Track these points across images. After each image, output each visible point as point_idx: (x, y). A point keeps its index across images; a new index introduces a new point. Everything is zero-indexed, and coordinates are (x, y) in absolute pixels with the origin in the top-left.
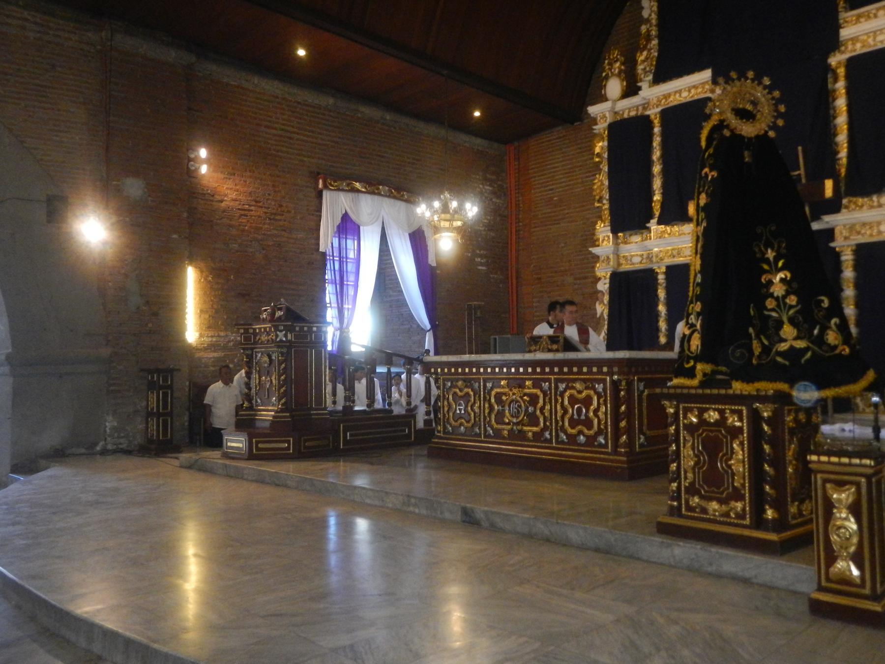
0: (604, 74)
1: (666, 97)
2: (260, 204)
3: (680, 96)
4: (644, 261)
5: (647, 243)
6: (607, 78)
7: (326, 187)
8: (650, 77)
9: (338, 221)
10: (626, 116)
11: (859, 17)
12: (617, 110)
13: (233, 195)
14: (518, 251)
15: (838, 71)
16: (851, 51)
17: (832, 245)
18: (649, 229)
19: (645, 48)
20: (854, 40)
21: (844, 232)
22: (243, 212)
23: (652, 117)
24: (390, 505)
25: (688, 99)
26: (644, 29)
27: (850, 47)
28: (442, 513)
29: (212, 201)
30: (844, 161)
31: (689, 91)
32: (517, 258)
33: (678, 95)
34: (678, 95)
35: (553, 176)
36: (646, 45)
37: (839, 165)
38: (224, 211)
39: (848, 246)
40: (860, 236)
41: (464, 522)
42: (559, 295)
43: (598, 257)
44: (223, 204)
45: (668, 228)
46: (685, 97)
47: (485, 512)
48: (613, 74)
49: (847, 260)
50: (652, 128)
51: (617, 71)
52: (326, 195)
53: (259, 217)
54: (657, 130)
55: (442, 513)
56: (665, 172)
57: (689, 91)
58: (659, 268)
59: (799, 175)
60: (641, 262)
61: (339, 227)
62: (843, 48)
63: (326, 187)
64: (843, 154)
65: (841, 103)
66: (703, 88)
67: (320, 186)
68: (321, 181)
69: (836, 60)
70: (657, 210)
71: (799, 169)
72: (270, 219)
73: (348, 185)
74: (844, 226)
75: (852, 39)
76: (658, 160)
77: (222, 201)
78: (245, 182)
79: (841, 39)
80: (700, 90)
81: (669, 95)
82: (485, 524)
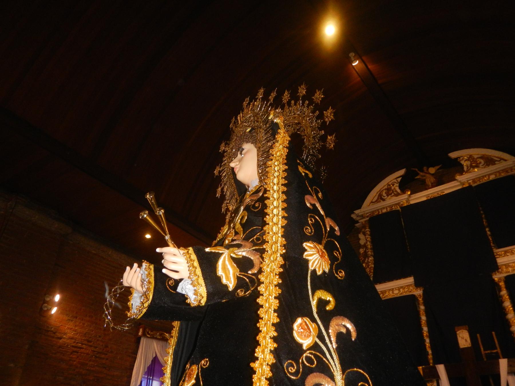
2: (91, 344)
3: (393, 292)
7: (144, 335)
9: (149, 362)
11: (506, 252)
13: (71, 334)
15: (501, 284)
16: (507, 272)
20: (507, 266)
22: (75, 349)
25: (399, 295)
26: (362, 251)
27: (505, 270)
29: (53, 337)
31: (399, 290)
34: (391, 292)
36: (364, 260)
38: (60, 347)
44: (61, 341)
46: (396, 293)
52: (143, 341)
53: (88, 354)
57: (399, 290)
59: (497, 353)
61: (148, 368)
62: (500, 270)
63: (144, 335)
66: (409, 289)
67: (140, 334)
68: (141, 330)
71: (496, 349)
72: (96, 357)
73: (161, 335)
75: (505, 265)
77: (61, 338)
78: (84, 324)
79: (499, 264)
80: (406, 290)
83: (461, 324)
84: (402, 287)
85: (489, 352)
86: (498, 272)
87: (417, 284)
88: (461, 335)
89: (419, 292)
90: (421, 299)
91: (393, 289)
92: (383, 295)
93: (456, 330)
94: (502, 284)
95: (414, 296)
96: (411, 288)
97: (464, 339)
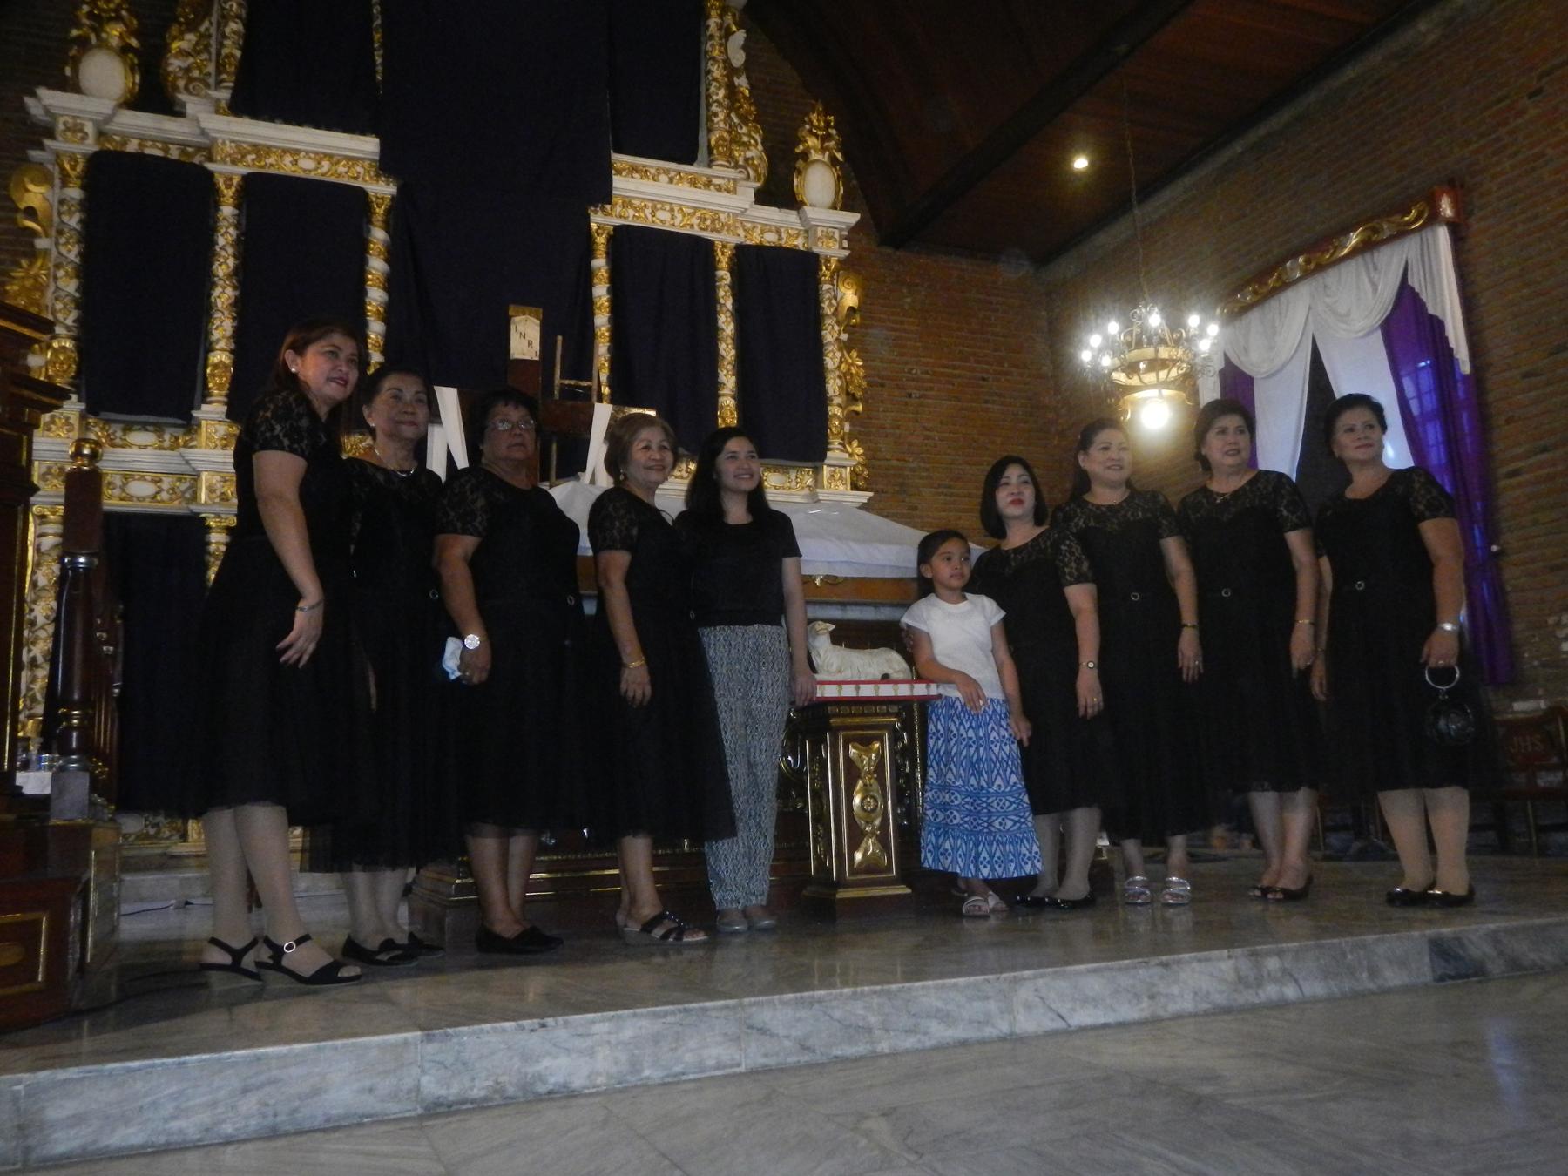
0: (75, 33)
1: (260, 150)
3: (295, 162)
4: (164, 496)
5: (191, 454)
6: (84, 44)
8: (224, 95)
10: (132, 147)
12: (113, 127)
19: (192, 26)
20: (627, 203)
23: (221, 182)
24: (1187, 1005)
25: (312, 176)
27: (618, 209)
28: (1373, 973)
33: (288, 159)
41: (1441, 979)
46: (306, 167)
47: (1494, 938)
48: (103, 44)
50: (217, 206)
54: (227, 210)
55: (1373, 973)
56: (241, 308)
58: (218, 515)
59: (590, 388)
60: (153, 498)
65: (601, 292)
69: (601, 221)
70: (218, 385)
76: (229, 276)
80: (341, 169)
81: (269, 150)
82: (1496, 967)
83: (527, 301)
84: (331, 156)
85: (572, 382)
86: (603, 209)
87: (386, 165)
88: (520, 328)
89: (383, 190)
90: (381, 211)
91: (297, 152)
92: (259, 158)
93: (511, 313)
94: (601, 240)
95: (362, 194)
96: (359, 169)
97: (525, 337)
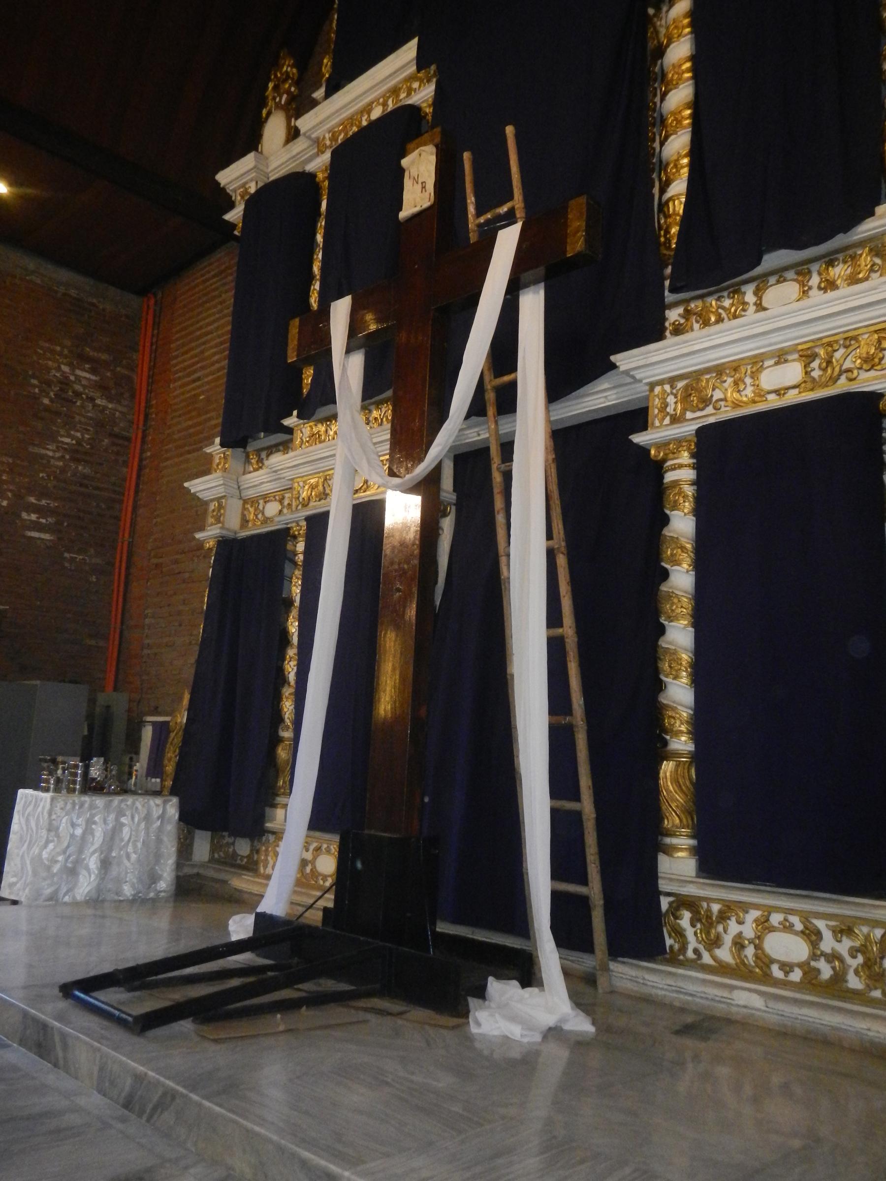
14: (135, 508)
17: (638, 439)
18: (289, 431)
21: (671, 400)
30: (678, 207)
31: (385, 104)
32: (133, 524)
35: (202, 352)
37: (667, 216)
39: (679, 442)
40: (710, 410)
42: (184, 602)
43: (206, 503)
45: (322, 428)
49: (676, 483)
51: (285, 97)
64: (679, 187)
74: (672, 381)
88: (414, 172)
